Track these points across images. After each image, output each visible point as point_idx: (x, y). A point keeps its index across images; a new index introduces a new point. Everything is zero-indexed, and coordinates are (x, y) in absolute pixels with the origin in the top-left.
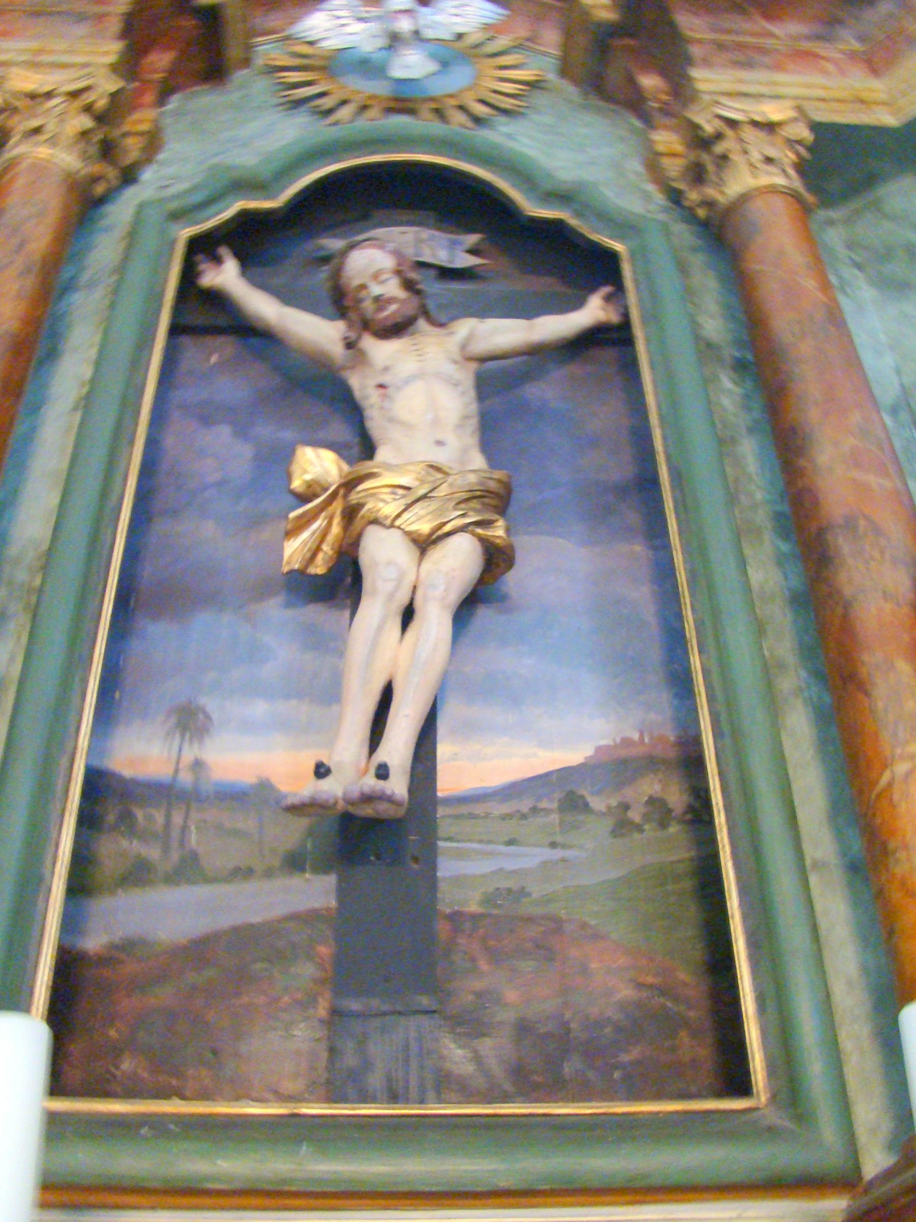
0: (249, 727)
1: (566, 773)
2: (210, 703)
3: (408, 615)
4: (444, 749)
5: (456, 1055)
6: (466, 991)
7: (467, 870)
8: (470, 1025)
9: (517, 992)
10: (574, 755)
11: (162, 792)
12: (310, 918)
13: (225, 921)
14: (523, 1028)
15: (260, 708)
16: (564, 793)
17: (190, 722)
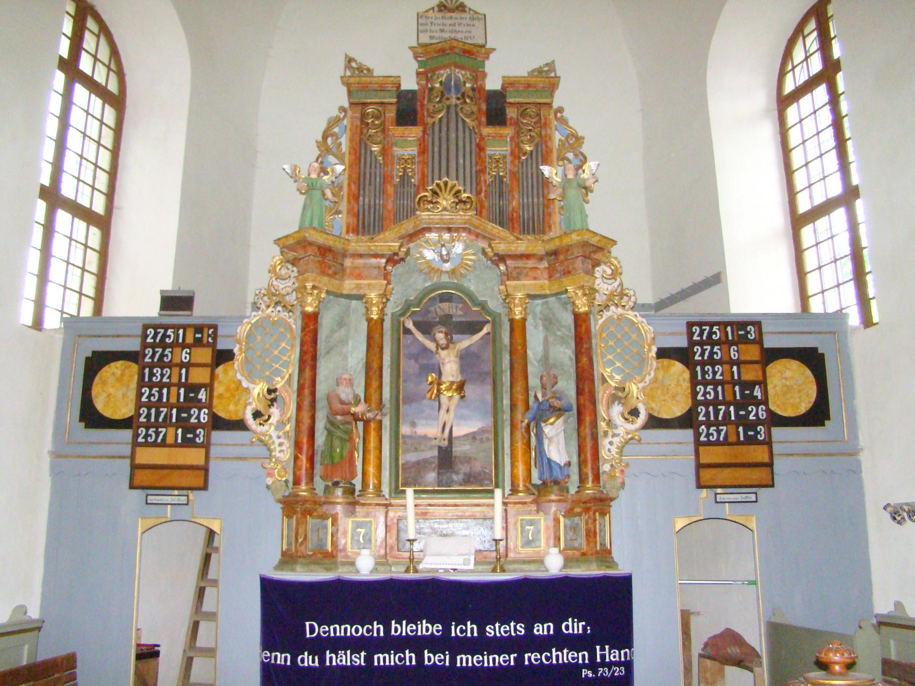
0: (423, 425)
1: (474, 433)
2: (416, 421)
3: (448, 411)
4: (454, 429)
5: (455, 477)
6: (456, 468)
7: (459, 449)
8: (457, 473)
9: (464, 469)
10: (475, 429)
11: (410, 437)
12: (434, 457)
13: (421, 458)
14: (465, 474)
15: (424, 422)
16: (473, 437)
17: (413, 424)
